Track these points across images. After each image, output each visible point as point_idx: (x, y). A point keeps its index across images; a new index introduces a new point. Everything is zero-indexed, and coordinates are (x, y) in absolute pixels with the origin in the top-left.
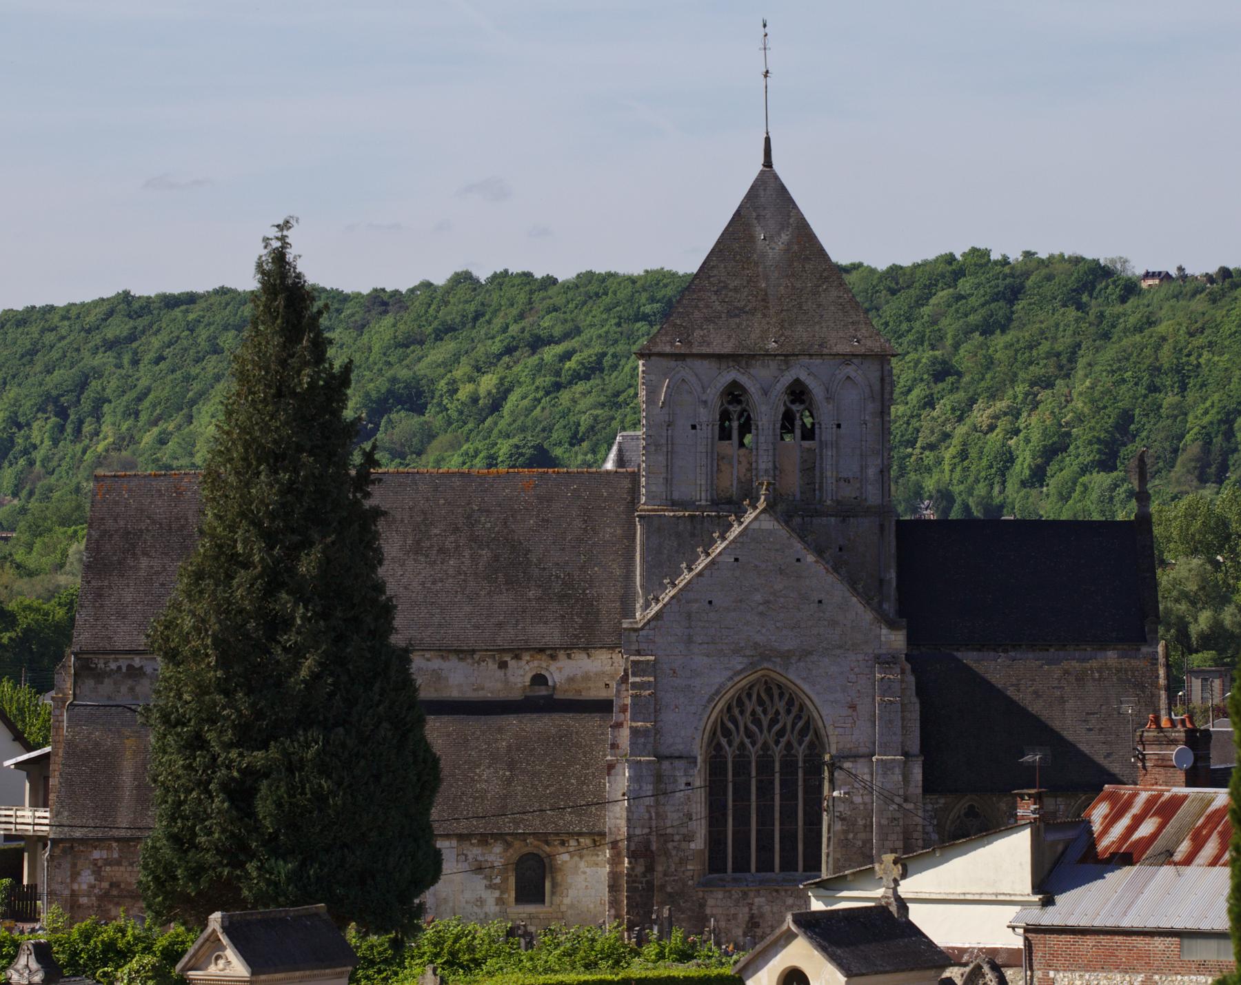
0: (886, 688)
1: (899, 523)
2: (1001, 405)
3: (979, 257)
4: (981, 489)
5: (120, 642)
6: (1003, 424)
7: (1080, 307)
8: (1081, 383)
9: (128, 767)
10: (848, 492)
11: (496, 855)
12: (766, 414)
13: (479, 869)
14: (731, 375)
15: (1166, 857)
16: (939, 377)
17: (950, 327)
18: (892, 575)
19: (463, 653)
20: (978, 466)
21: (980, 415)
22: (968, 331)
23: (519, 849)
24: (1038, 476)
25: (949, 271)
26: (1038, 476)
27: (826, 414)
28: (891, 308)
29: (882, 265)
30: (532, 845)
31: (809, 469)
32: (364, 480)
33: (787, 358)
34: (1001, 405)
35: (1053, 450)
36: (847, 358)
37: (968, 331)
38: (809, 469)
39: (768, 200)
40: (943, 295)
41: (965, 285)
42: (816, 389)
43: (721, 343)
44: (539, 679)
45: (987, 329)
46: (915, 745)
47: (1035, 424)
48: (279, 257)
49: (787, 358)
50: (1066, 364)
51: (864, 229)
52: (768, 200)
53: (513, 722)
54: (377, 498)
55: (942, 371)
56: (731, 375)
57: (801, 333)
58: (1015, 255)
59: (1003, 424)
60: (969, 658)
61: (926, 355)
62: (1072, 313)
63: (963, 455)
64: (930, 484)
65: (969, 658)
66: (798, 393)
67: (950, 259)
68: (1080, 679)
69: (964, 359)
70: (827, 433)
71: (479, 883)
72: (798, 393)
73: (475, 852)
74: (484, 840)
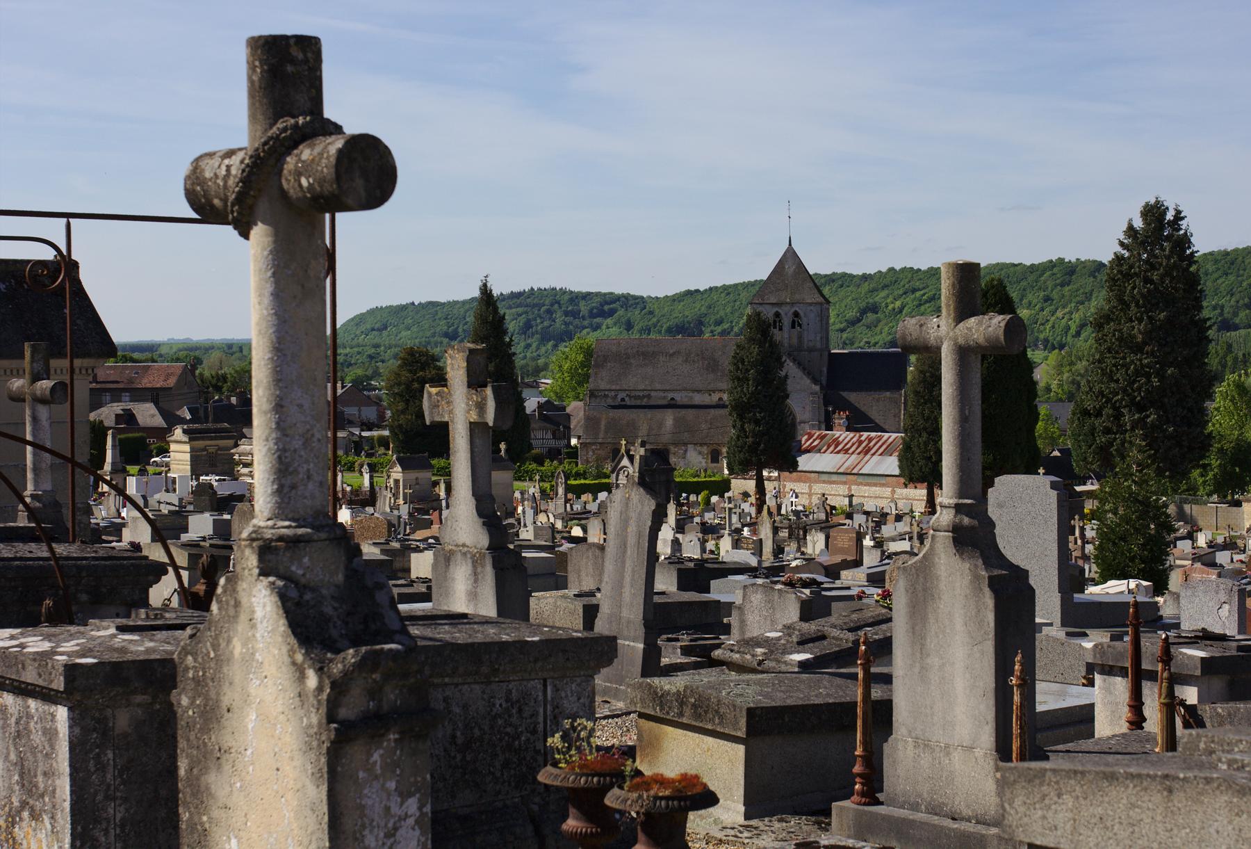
0: (813, 402)
1: (831, 355)
2: (1066, 310)
3: (1061, 260)
4: (1059, 338)
5: (602, 387)
6: (1067, 317)
7: (1095, 277)
8: (1094, 303)
9: (603, 423)
10: (811, 344)
11: (705, 450)
12: (786, 322)
13: (700, 453)
14: (775, 309)
15: (819, 451)
16: (1046, 301)
17: (1050, 284)
18: (825, 369)
19: (699, 391)
20: (1058, 331)
21: (1059, 314)
22: (1056, 286)
23: (712, 447)
24: (1078, 334)
25: (1051, 265)
26: (1078, 334)
27: (804, 321)
28: (1031, 278)
29: (1028, 264)
30: (715, 447)
31: (800, 337)
32: (509, 345)
33: (792, 304)
34: (1066, 310)
35: (1082, 326)
36: (811, 304)
37: (1056, 286)
38: (800, 337)
39: (790, 256)
40: (1048, 274)
41: (1055, 270)
42: (802, 314)
43: (773, 300)
44: (720, 399)
45: (1062, 285)
46: (822, 419)
47: (1076, 316)
48: (485, 285)
49: (792, 304)
50: (1088, 297)
51: (816, 264)
52: (790, 256)
53: (712, 411)
54: (513, 349)
55: (1047, 299)
56: (775, 309)
57: (797, 297)
58: (1073, 260)
59: (1067, 317)
60: (845, 394)
61: (1042, 294)
62: (1092, 279)
63: (1053, 327)
64: (1042, 336)
65: (845, 394)
66: (796, 314)
67: (1051, 261)
68: (878, 400)
69: (1055, 295)
70: (804, 327)
71: (700, 458)
72: (796, 314)
73: (699, 448)
74: (701, 445)
